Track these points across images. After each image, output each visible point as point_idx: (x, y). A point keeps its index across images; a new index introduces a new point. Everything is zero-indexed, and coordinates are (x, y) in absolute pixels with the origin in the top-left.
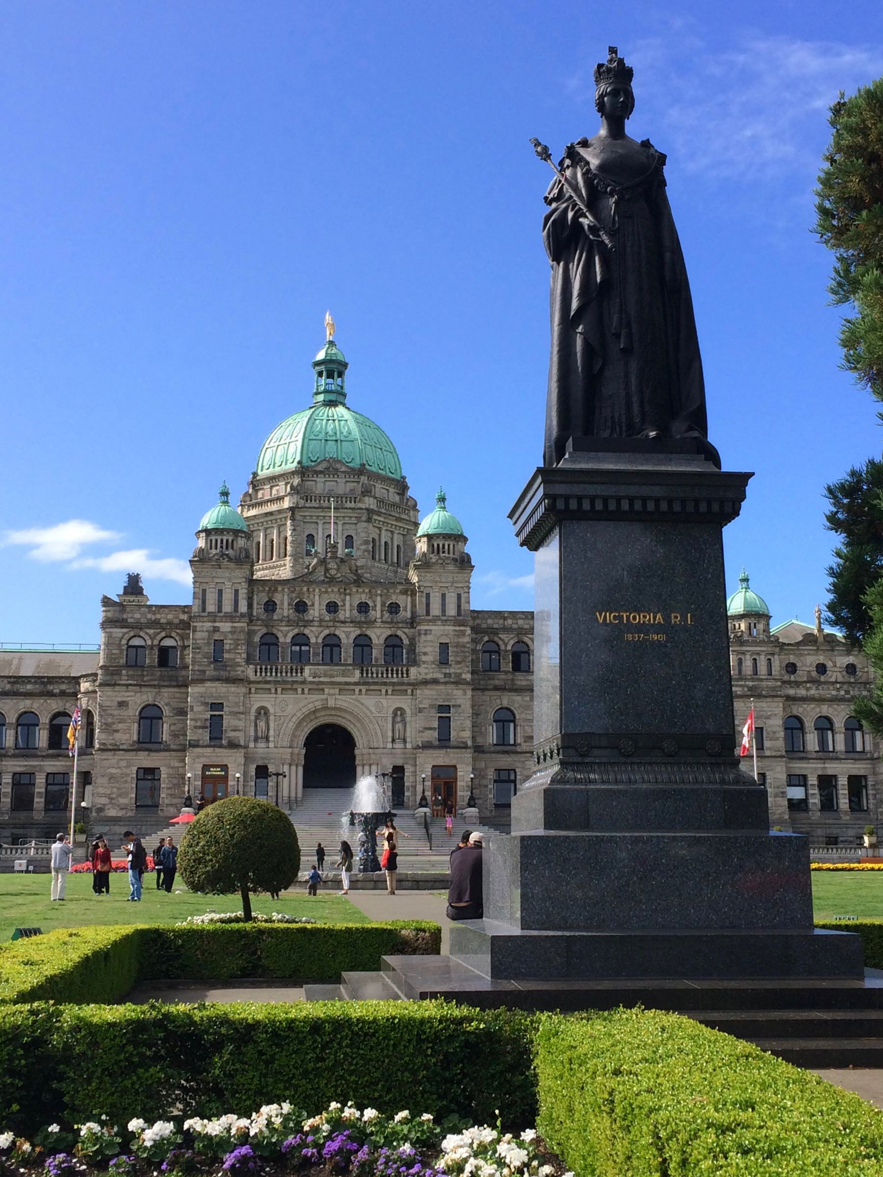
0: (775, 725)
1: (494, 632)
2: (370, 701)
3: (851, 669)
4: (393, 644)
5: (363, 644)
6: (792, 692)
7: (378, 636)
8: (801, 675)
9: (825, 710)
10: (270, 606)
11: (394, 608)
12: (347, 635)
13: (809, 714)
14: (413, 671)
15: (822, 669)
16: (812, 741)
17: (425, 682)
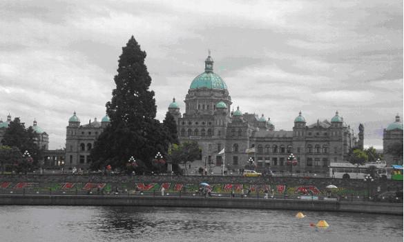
0: (303, 146)
1: (234, 127)
2: (204, 143)
3: (326, 134)
4: (209, 131)
5: (204, 130)
6: (310, 139)
7: (206, 129)
8: (312, 135)
9: (318, 143)
10: (183, 123)
11: (210, 123)
12: (200, 129)
13: (314, 144)
14: (213, 137)
15: (318, 134)
16: (314, 150)
17: (215, 139)
